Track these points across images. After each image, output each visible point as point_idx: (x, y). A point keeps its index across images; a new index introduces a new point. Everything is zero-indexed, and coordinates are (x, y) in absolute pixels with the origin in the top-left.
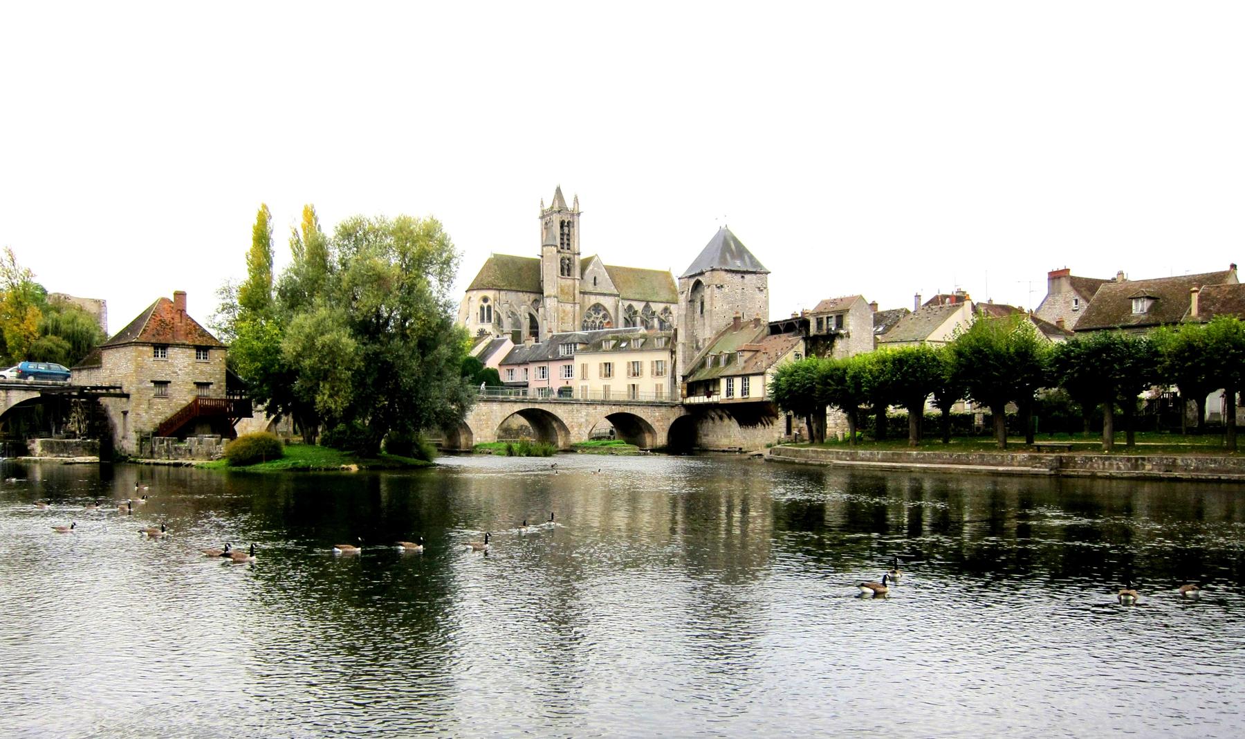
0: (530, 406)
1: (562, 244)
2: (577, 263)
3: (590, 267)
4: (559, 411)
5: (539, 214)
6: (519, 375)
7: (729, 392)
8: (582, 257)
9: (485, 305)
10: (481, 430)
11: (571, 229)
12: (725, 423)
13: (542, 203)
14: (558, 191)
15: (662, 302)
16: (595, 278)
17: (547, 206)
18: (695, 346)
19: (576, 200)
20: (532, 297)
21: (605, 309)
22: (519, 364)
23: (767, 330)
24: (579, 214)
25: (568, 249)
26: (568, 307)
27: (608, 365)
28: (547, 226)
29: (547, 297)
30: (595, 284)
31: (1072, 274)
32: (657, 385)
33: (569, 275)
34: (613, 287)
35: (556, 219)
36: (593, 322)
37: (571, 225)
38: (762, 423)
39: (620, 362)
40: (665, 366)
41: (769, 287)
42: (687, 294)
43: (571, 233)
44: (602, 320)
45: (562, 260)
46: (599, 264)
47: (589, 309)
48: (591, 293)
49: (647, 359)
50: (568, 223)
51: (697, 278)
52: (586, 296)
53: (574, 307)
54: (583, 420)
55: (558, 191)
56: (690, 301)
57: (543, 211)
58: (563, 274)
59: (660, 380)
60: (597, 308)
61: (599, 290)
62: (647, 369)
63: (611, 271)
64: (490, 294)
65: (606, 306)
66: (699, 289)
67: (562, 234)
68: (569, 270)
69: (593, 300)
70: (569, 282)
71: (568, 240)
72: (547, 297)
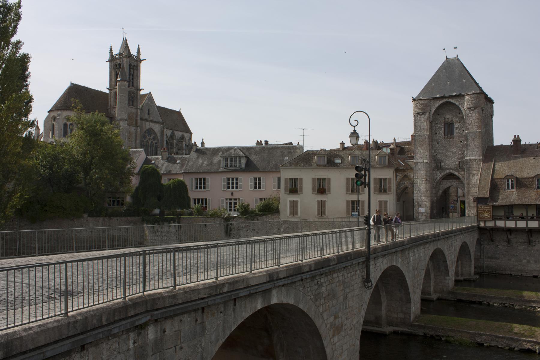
5: (108, 57)
8: (142, 93)
11: (135, 72)
13: (111, 49)
14: (125, 42)
15: (181, 131)
16: (149, 110)
17: (116, 52)
21: (155, 133)
24: (141, 61)
25: (133, 86)
26: (133, 129)
27: (321, 181)
34: (159, 118)
35: (125, 63)
36: (147, 141)
37: (135, 68)
40: (390, 183)
43: (135, 74)
47: (145, 132)
48: (146, 120)
51: (445, 100)
52: (143, 122)
53: (136, 130)
55: (125, 42)
57: (112, 56)
59: (383, 197)
60: (150, 131)
61: (151, 118)
65: (156, 130)
67: (129, 74)
68: (133, 102)
71: (133, 79)
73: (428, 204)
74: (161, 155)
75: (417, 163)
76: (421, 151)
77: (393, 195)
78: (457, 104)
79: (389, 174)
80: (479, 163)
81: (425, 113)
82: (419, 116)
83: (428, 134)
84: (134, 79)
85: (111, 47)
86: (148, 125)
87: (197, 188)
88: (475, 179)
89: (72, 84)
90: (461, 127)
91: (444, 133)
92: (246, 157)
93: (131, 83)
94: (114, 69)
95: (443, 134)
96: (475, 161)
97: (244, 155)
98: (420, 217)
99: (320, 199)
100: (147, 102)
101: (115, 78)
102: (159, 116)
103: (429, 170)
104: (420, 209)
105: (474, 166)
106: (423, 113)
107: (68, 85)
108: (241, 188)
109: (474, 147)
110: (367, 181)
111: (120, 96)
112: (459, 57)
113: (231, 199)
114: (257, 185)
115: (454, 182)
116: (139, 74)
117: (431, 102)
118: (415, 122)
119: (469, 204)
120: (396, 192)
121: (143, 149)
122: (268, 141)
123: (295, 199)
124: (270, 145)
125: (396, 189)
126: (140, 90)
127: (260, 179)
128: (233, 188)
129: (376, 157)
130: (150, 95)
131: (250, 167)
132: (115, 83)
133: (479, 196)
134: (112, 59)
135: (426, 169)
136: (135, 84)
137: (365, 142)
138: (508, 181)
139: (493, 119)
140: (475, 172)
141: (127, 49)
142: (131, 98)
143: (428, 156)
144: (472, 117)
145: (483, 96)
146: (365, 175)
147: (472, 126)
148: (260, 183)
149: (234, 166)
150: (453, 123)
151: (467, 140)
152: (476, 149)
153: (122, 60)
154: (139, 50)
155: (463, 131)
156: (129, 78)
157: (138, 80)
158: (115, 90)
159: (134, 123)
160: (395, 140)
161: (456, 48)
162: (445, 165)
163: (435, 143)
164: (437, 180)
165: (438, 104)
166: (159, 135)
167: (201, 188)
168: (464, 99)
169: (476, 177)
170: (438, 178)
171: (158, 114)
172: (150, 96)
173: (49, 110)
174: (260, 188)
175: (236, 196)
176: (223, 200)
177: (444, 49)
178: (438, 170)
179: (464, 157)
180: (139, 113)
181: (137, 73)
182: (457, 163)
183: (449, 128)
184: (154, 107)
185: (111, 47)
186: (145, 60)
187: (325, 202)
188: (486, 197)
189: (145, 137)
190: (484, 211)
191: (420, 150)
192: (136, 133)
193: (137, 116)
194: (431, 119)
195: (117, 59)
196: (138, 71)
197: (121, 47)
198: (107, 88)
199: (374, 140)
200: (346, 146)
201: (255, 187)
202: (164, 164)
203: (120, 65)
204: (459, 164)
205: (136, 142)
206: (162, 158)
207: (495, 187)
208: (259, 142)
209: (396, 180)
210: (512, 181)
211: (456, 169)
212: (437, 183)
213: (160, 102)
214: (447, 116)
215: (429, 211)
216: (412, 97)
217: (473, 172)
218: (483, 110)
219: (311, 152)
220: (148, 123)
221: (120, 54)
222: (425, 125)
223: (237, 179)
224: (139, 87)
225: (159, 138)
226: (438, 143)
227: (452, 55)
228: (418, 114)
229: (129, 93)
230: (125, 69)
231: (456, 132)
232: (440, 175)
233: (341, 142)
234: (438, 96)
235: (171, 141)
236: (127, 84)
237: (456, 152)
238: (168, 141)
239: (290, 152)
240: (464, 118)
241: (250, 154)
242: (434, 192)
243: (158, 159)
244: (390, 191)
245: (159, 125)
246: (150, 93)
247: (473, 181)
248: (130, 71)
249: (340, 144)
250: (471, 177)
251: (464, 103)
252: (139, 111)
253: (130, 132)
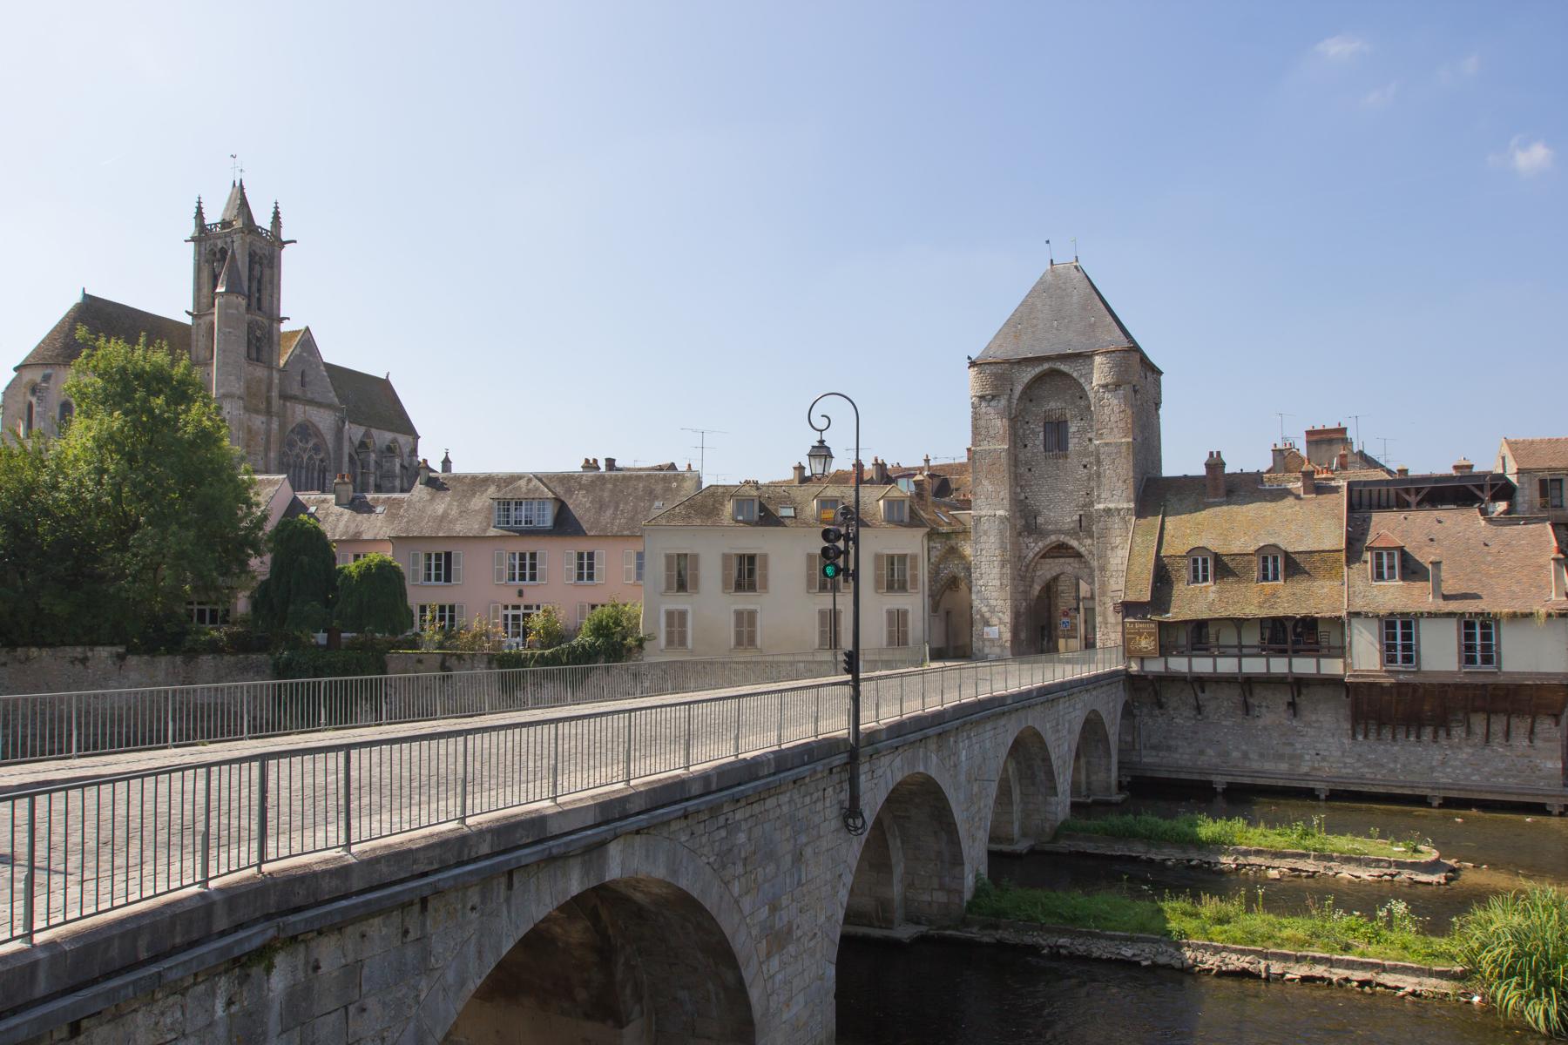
5: (190, 229)
11: (267, 272)
13: (199, 209)
16: (303, 372)
17: (213, 216)
21: (318, 434)
25: (259, 309)
26: (258, 421)
34: (332, 394)
36: (297, 456)
37: (265, 262)
40: (914, 567)
43: (266, 278)
44: (312, 453)
47: (292, 431)
51: (1046, 366)
52: (288, 404)
53: (269, 423)
58: (249, 356)
59: (898, 601)
60: (306, 430)
61: (309, 395)
65: (321, 426)
68: (258, 350)
71: (259, 291)
73: (1007, 618)
74: (334, 492)
75: (981, 517)
76: (990, 488)
77: (920, 595)
78: (1075, 375)
79: (911, 543)
80: (1127, 518)
81: (999, 396)
82: (983, 404)
83: (1006, 447)
84: (263, 292)
85: (199, 203)
86: (299, 413)
87: (429, 578)
88: (1118, 559)
89: (86, 296)
90: (1085, 431)
91: (1045, 446)
92: (557, 499)
93: (254, 301)
94: (207, 262)
95: (1042, 449)
96: (1119, 514)
97: (550, 495)
98: (987, 650)
99: (740, 607)
100: (297, 352)
101: (211, 286)
102: (332, 389)
103: (1008, 534)
104: (986, 629)
105: (1116, 526)
106: (994, 397)
107: (77, 298)
108: (543, 578)
109: (1115, 479)
110: (852, 567)
111: (224, 334)
112: (1081, 263)
113: (516, 607)
114: (585, 571)
115: (1069, 564)
116: (276, 278)
117: (1012, 369)
118: (976, 417)
119: (1105, 617)
120: (930, 590)
121: (285, 476)
122: (614, 460)
123: (681, 607)
124: (620, 470)
125: (929, 581)
126: (281, 320)
127: (591, 556)
128: (522, 577)
129: (881, 502)
130: (307, 335)
131: (565, 524)
132: (211, 300)
133: (1127, 599)
134: (203, 235)
135: (1001, 532)
136: (265, 304)
137: (854, 465)
138: (1195, 561)
139: (1161, 412)
140: (1118, 540)
141: (245, 211)
142: (254, 342)
143: (1006, 502)
144: (1111, 412)
145: (1138, 357)
146: (847, 553)
147: (1112, 429)
148: (591, 566)
149: (526, 523)
150: (1066, 422)
151: (1099, 462)
152: (1120, 484)
153: (229, 240)
154: (276, 216)
155: (1090, 440)
156: (249, 287)
157: (276, 296)
158: (209, 318)
159: (263, 406)
160: (927, 460)
162: (1046, 523)
163: (1022, 470)
164: (1027, 560)
165: (1029, 374)
166: (329, 438)
167: (438, 578)
168: (1092, 363)
169: (1120, 552)
170: (1031, 555)
171: (329, 385)
172: (306, 337)
173: (18, 362)
174: (591, 577)
175: (531, 597)
176: (496, 610)
177: (1048, 242)
178: (1030, 534)
179: (1092, 504)
180: (276, 381)
181: (272, 276)
182: (1076, 517)
183: (1056, 433)
184: (318, 367)
185: (199, 203)
186: (295, 242)
187: (752, 615)
188: (1142, 600)
189: (291, 445)
190: (1140, 634)
191: (987, 485)
192: (268, 432)
193: (269, 389)
194: (1013, 411)
195: (218, 236)
196: (276, 270)
197: (228, 204)
198: (187, 312)
199: (876, 460)
200: (808, 473)
201: (580, 577)
202: (341, 515)
203: (223, 252)
204: (1080, 520)
205: (266, 455)
206: (338, 499)
207: (1162, 578)
208: (591, 462)
209: (929, 560)
210: (1205, 561)
211: (1073, 533)
212: (1027, 566)
213: (333, 352)
214: (1053, 405)
215: (1009, 634)
216: (969, 358)
217: (1113, 540)
218: (1135, 391)
219: (720, 490)
220: (299, 408)
221: (225, 224)
222: (999, 425)
223: (533, 556)
224: (275, 312)
225: (330, 446)
226: (1030, 470)
227: (1064, 258)
228: (982, 398)
229: (249, 327)
230: (239, 264)
231: (1073, 444)
232: (1035, 547)
233: (797, 465)
234: (1030, 355)
235: (362, 457)
236: (244, 303)
237: (1072, 492)
238: (356, 457)
239: (668, 490)
240: (1092, 409)
241: (569, 491)
242: (1021, 589)
243: (324, 501)
244: (915, 586)
245: (331, 412)
246: (307, 329)
247: (1113, 561)
248: (251, 269)
249: (795, 468)
250: (1109, 552)
251: (1092, 373)
252: (276, 376)
253: (250, 430)
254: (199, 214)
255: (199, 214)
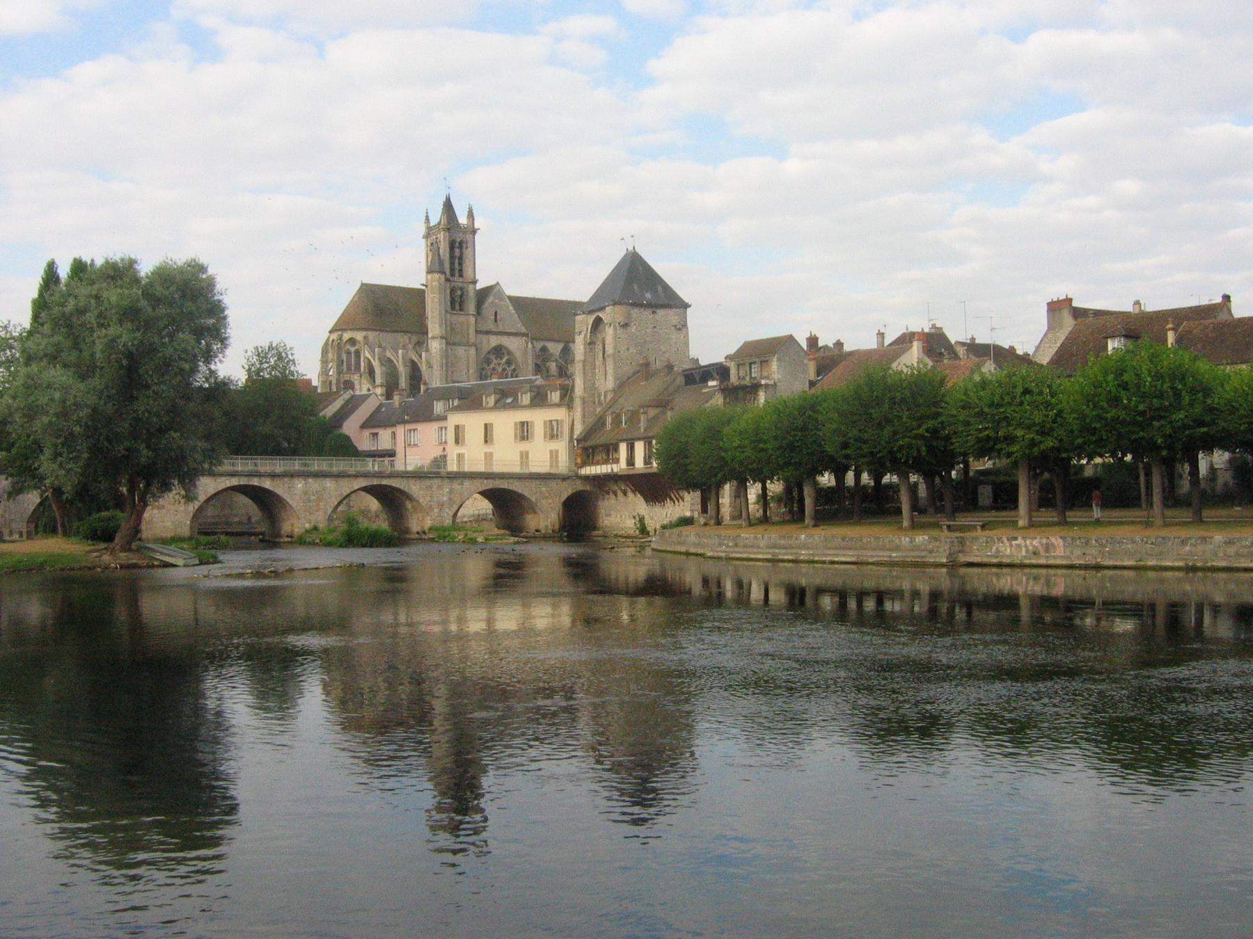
0: (375, 482)
1: (452, 269)
2: (472, 294)
3: (490, 299)
4: (413, 488)
5: (422, 230)
6: (385, 439)
7: (631, 462)
8: (479, 286)
9: (353, 349)
10: (310, 514)
11: (464, 251)
12: (630, 499)
16: (496, 313)
18: (597, 400)
19: (471, 215)
20: (414, 338)
21: (509, 353)
22: (385, 426)
23: (680, 380)
26: (460, 351)
28: (433, 248)
29: (433, 338)
30: (496, 321)
31: (1075, 304)
32: (551, 452)
33: (461, 310)
37: (464, 245)
38: (671, 499)
39: (505, 422)
41: (689, 324)
42: (586, 335)
44: (505, 366)
45: (453, 291)
46: (500, 294)
47: (489, 353)
48: (488, 333)
49: (538, 418)
50: (461, 243)
54: (445, 499)
56: (590, 344)
57: (429, 229)
58: (453, 308)
60: (499, 351)
61: (501, 329)
62: (539, 430)
63: (521, 304)
64: (359, 336)
66: (601, 328)
67: (452, 257)
69: (494, 341)
70: (462, 319)
71: (460, 264)
72: (433, 338)
85: (427, 213)
89: (362, 284)
136: (464, 274)
161: (623, 239)
171: (518, 319)
185: (427, 213)
246: (498, 283)
254: (427, 218)
255: (427, 218)
